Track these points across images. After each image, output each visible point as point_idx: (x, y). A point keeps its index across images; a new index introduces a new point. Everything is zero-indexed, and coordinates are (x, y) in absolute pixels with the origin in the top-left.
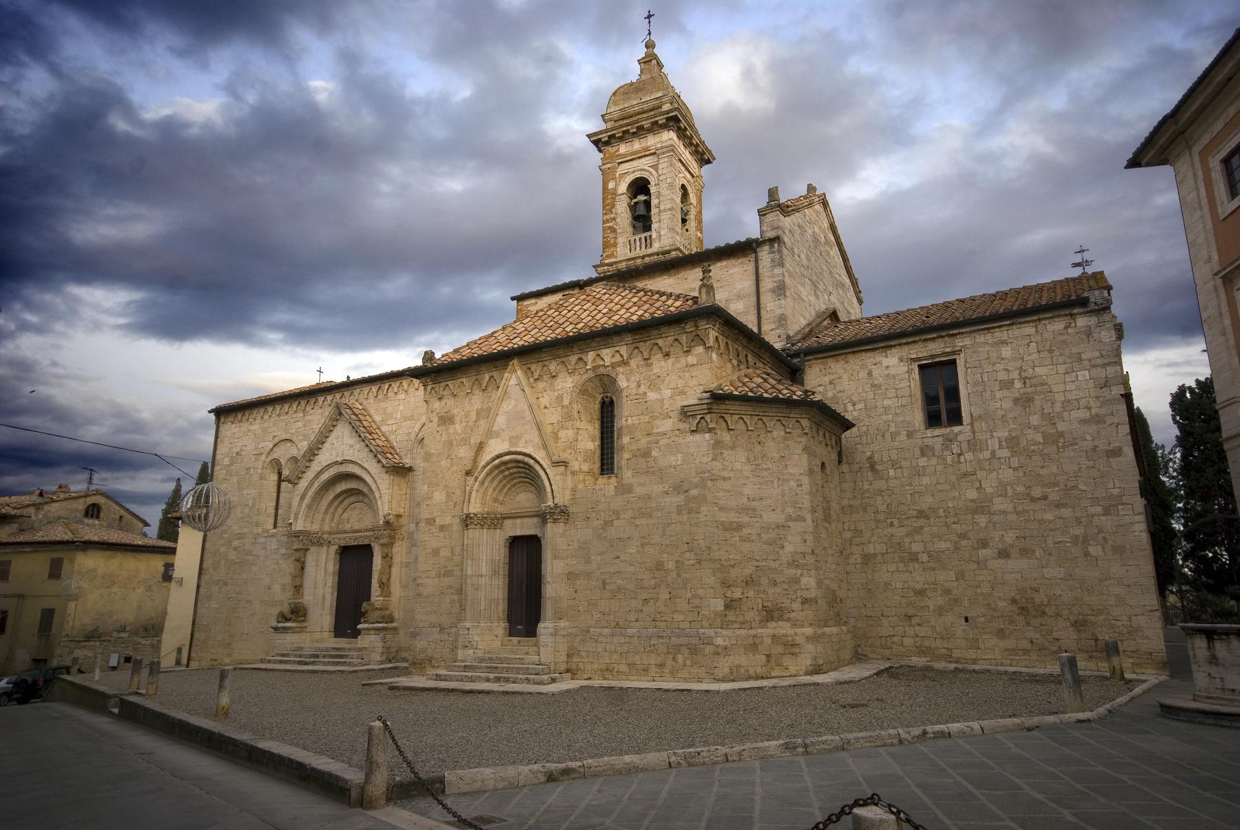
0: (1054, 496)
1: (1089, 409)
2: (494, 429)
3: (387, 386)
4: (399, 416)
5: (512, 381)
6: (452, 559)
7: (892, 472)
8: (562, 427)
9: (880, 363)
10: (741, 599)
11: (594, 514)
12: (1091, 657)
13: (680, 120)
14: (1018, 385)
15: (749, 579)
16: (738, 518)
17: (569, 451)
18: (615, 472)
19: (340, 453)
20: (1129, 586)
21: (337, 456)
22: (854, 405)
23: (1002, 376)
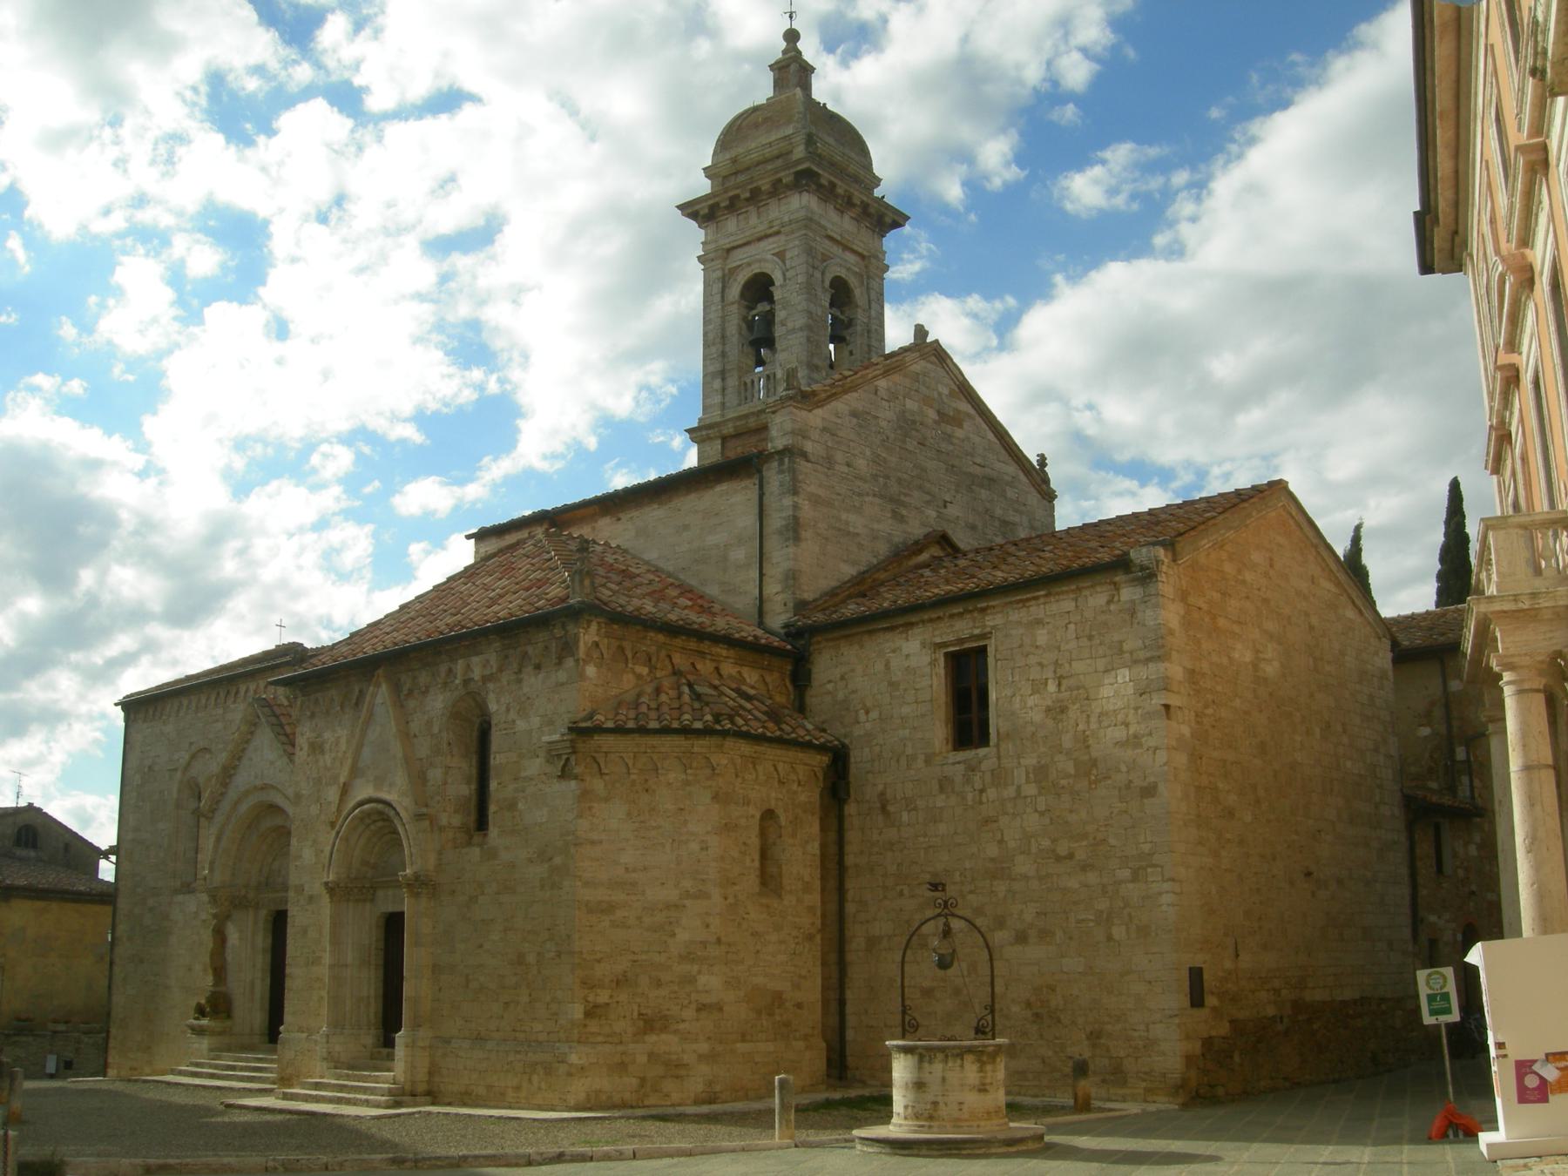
0: (1081, 855)
1: (1127, 725)
7: (905, 817)
9: (900, 649)
10: (608, 1004)
12: (1104, 1081)
13: (819, 174)
14: (1052, 687)
15: (620, 977)
16: (610, 895)
20: (1150, 982)
21: (256, 777)
22: (867, 713)
23: (1035, 674)
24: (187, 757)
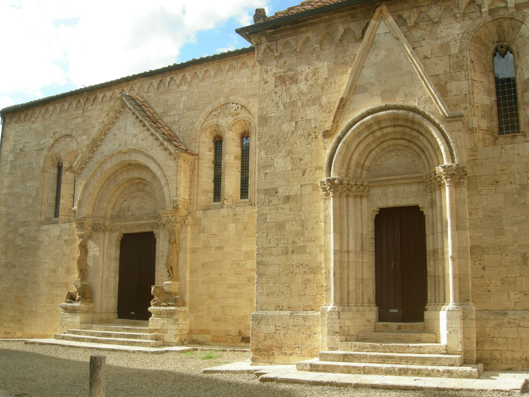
2: (359, 83)
3: (168, 79)
4: (181, 107)
5: (380, 28)
6: (303, 234)
8: (452, 78)
11: (505, 177)
17: (463, 105)
18: (522, 129)
19: (123, 143)
21: (120, 145)
24: (52, 141)
